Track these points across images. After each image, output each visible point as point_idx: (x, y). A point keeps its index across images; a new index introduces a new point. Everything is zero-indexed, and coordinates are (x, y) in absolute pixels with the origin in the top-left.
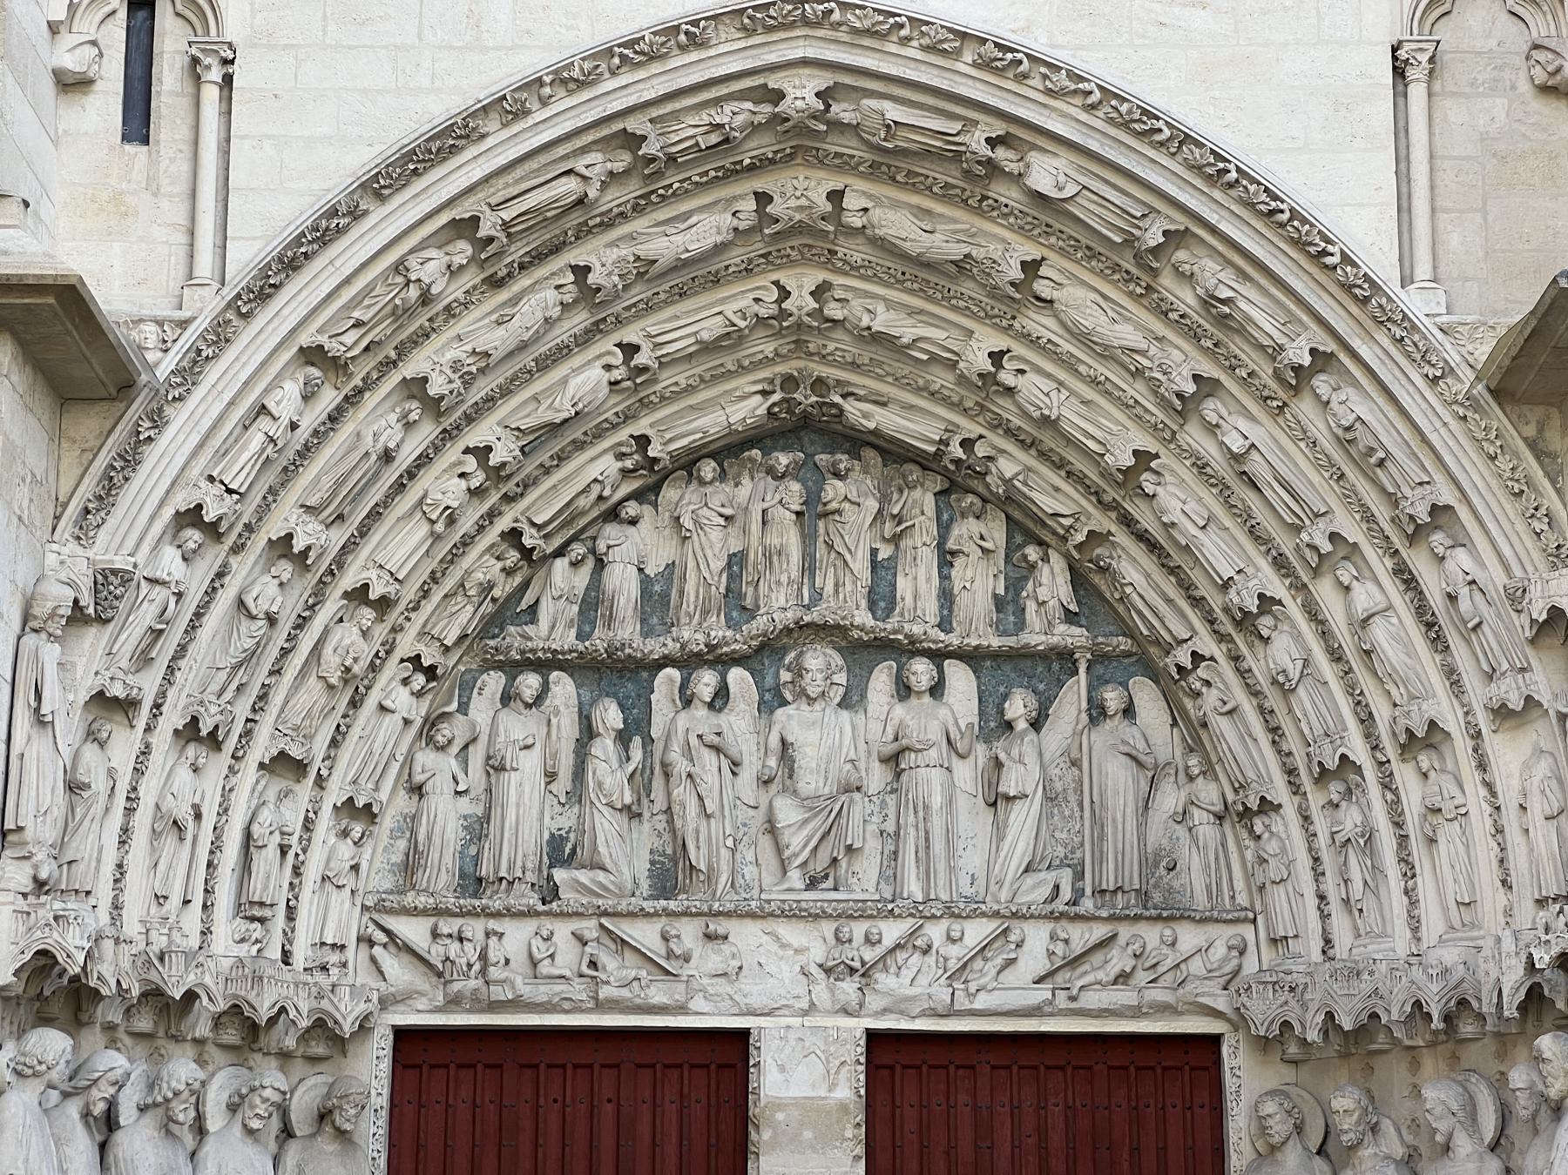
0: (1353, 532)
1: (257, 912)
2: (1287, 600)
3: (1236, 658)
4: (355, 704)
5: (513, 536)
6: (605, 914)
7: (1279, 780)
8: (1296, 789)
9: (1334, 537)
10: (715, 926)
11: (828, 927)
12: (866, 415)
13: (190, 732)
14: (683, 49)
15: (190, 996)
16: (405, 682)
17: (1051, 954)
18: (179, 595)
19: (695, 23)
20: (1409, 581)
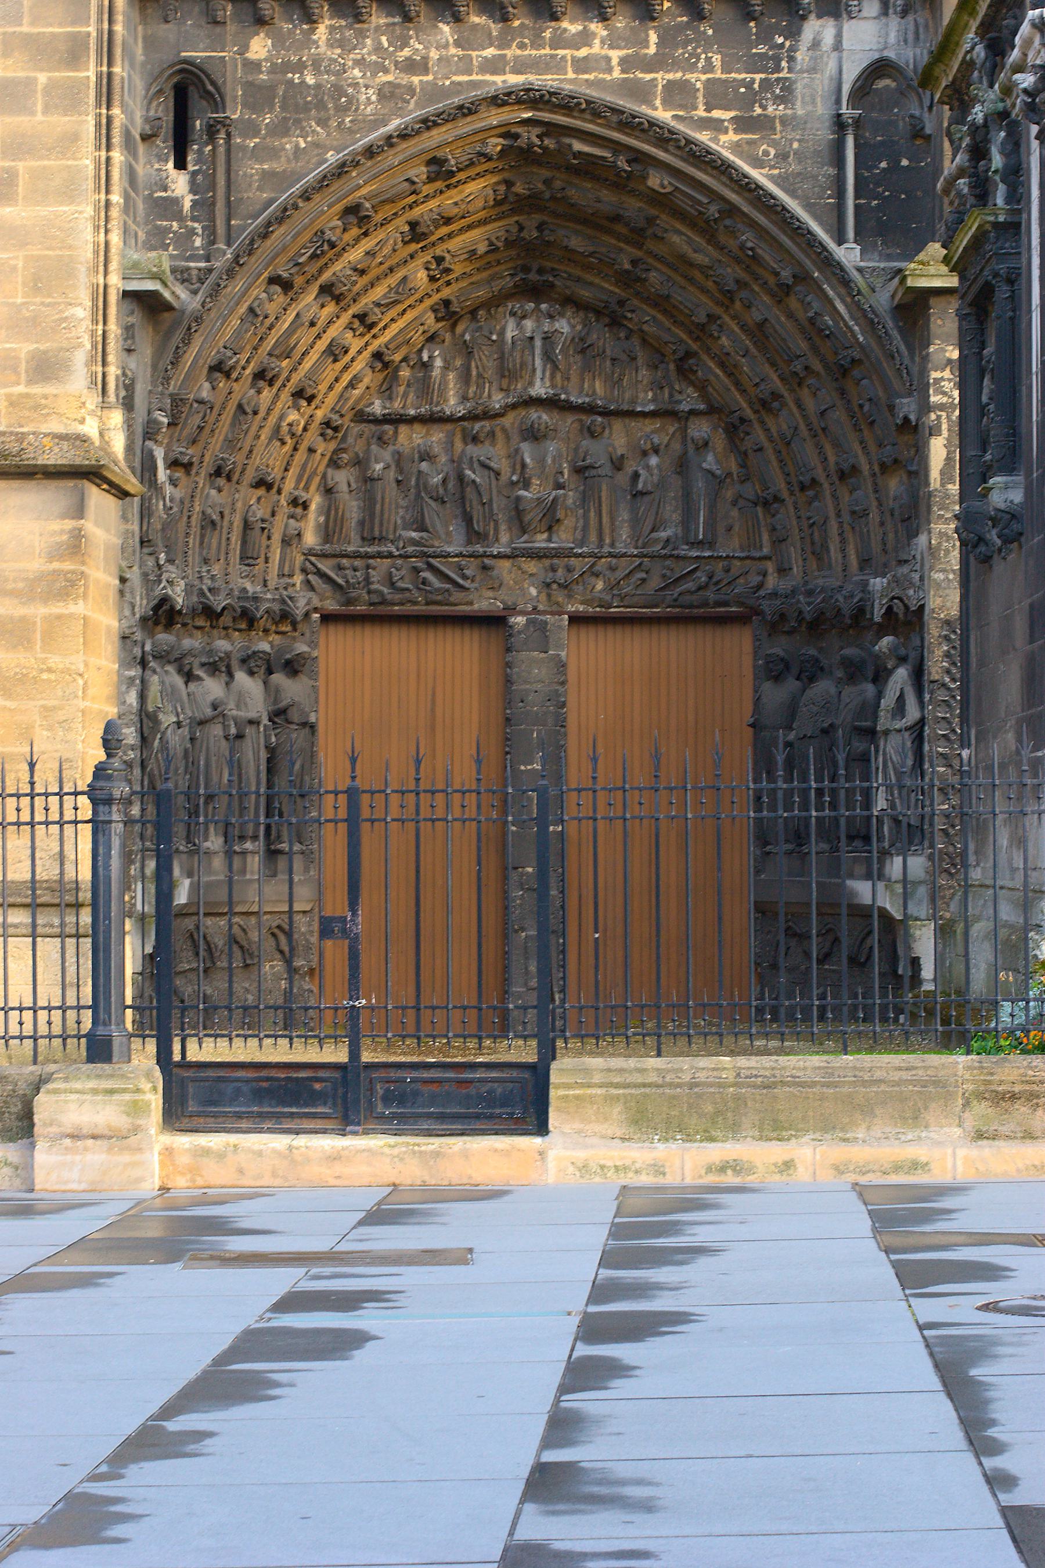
0: (817, 366)
1: (251, 561)
2: (786, 394)
3: (762, 423)
4: (295, 449)
5: (378, 356)
6: (429, 556)
7: (783, 485)
8: (792, 493)
9: (807, 368)
10: (486, 561)
11: (547, 562)
12: (567, 287)
13: (218, 472)
14: (465, 115)
15: (224, 609)
16: (322, 435)
17: (664, 576)
18: (212, 408)
19: (472, 103)
20: (842, 392)
